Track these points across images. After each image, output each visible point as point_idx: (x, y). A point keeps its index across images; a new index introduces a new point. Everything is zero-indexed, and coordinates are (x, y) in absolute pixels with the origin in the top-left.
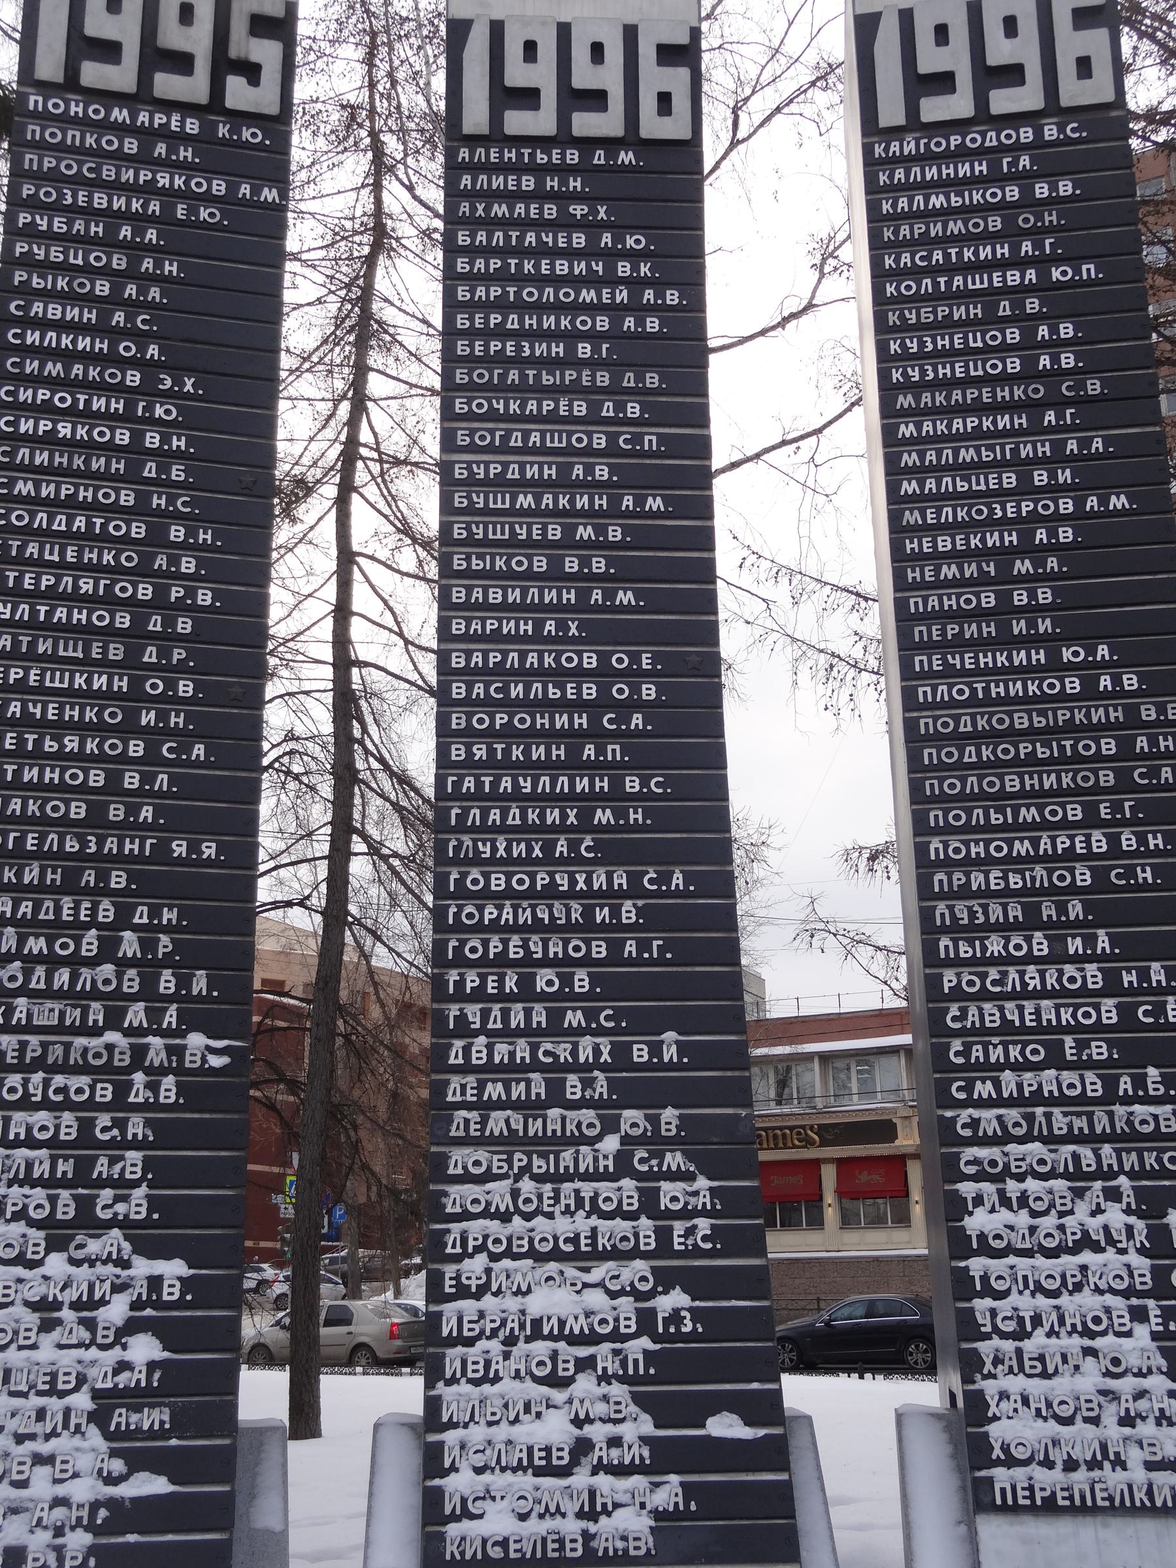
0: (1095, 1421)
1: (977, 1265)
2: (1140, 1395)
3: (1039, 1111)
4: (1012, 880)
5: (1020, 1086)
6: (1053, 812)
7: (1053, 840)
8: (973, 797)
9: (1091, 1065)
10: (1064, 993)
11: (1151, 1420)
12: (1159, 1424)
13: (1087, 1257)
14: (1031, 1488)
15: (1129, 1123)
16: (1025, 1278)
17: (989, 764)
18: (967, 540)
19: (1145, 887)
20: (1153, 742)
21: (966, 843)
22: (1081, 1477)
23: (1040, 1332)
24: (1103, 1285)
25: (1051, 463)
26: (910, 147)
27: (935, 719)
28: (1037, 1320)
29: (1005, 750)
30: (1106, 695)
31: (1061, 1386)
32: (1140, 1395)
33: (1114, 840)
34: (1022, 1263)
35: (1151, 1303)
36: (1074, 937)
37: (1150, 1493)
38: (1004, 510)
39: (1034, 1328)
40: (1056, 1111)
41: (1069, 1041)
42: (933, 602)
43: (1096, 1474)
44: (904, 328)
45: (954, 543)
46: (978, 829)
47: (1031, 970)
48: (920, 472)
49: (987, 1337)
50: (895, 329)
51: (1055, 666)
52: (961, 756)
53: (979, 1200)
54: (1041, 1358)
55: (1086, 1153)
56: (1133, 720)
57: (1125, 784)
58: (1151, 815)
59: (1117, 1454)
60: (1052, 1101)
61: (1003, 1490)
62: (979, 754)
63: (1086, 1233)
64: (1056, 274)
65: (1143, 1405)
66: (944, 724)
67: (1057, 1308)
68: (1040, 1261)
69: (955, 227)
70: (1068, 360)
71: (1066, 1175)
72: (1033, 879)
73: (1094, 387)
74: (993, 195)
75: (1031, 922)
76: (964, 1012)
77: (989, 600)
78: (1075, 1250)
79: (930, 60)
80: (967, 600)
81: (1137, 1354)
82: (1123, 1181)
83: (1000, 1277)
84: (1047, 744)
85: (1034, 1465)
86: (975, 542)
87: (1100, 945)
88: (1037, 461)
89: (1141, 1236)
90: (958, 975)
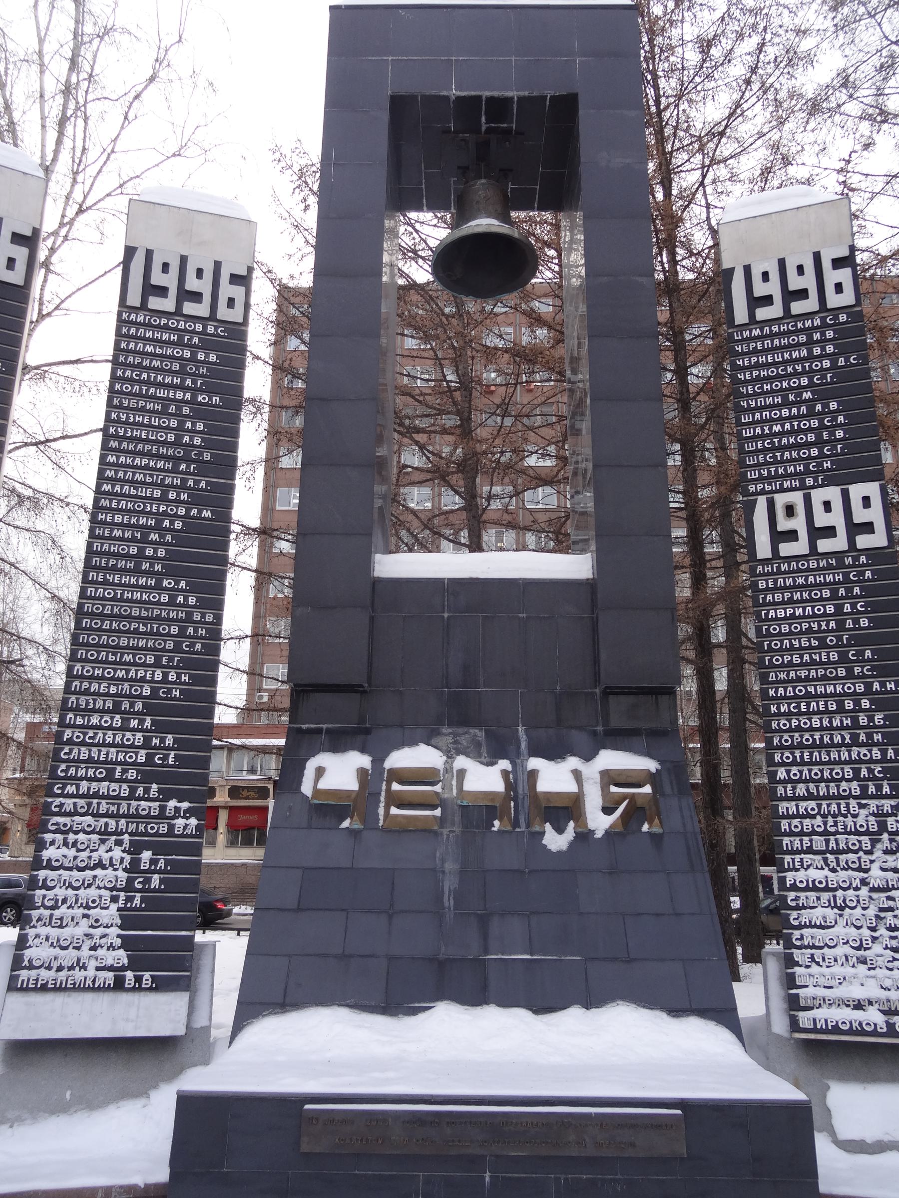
0: (78, 948)
1: (42, 874)
2: (104, 936)
3: (95, 801)
4: (112, 689)
5: (89, 789)
6: (140, 658)
7: (137, 671)
8: (103, 646)
9: (126, 781)
10: (122, 745)
11: (105, 948)
12: (108, 949)
13: (99, 872)
14: (37, 980)
15: (137, 809)
16: (65, 880)
17: (115, 631)
18: (130, 519)
19: (175, 699)
20: (196, 631)
21: (94, 668)
22: (63, 974)
23: (65, 906)
24: (101, 885)
25: (183, 487)
26: (141, 319)
27: (93, 605)
28: (64, 901)
29: (124, 625)
30: (180, 605)
31: (66, 932)
32: (104, 936)
33: (165, 675)
34: (65, 874)
35: (122, 894)
36: (134, 719)
37: (94, 981)
38: (151, 507)
39: (62, 904)
40: (104, 802)
41: (119, 769)
42: (106, 547)
43: (72, 972)
44: (121, 407)
45: (123, 519)
46: (101, 662)
47: (110, 733)
48: (113, 481)
49: (38, 908)
50: (116, 407)
51: (158, 587)
52: (102, 625)
53: (52, 843)
54: (61, 919)
55: (112, 823)
56: (189, 619)
57: (177, 649)
58: (186, 664)
59: (84, 963)
60: (103, 797)
61: (23, 981)
62: (111, 625)
63: (101, 860)
64: (200, 398)
65: (103, 941)
66: (97, 608)
67: (77, 895)
68: (75, 873)
69: (156, 364)
70: (197, 441)
71: (99, 833)
72: (122, 689)
73: (207, 456)
74: (177, 352)
75: (116, 709)
76: (71, 750)
77: (134, 550)
78: (92, 869)
79: (158, 278)
80: (123, 549)
81: (108, 917)
82: (126, 837)
83: (52, 880)
84: (145, 625)
85: (42, 969)
86: (133, 520)
87: (146, 724)
88: (172, 486)
89: (126, 864)
90: (73, 732)
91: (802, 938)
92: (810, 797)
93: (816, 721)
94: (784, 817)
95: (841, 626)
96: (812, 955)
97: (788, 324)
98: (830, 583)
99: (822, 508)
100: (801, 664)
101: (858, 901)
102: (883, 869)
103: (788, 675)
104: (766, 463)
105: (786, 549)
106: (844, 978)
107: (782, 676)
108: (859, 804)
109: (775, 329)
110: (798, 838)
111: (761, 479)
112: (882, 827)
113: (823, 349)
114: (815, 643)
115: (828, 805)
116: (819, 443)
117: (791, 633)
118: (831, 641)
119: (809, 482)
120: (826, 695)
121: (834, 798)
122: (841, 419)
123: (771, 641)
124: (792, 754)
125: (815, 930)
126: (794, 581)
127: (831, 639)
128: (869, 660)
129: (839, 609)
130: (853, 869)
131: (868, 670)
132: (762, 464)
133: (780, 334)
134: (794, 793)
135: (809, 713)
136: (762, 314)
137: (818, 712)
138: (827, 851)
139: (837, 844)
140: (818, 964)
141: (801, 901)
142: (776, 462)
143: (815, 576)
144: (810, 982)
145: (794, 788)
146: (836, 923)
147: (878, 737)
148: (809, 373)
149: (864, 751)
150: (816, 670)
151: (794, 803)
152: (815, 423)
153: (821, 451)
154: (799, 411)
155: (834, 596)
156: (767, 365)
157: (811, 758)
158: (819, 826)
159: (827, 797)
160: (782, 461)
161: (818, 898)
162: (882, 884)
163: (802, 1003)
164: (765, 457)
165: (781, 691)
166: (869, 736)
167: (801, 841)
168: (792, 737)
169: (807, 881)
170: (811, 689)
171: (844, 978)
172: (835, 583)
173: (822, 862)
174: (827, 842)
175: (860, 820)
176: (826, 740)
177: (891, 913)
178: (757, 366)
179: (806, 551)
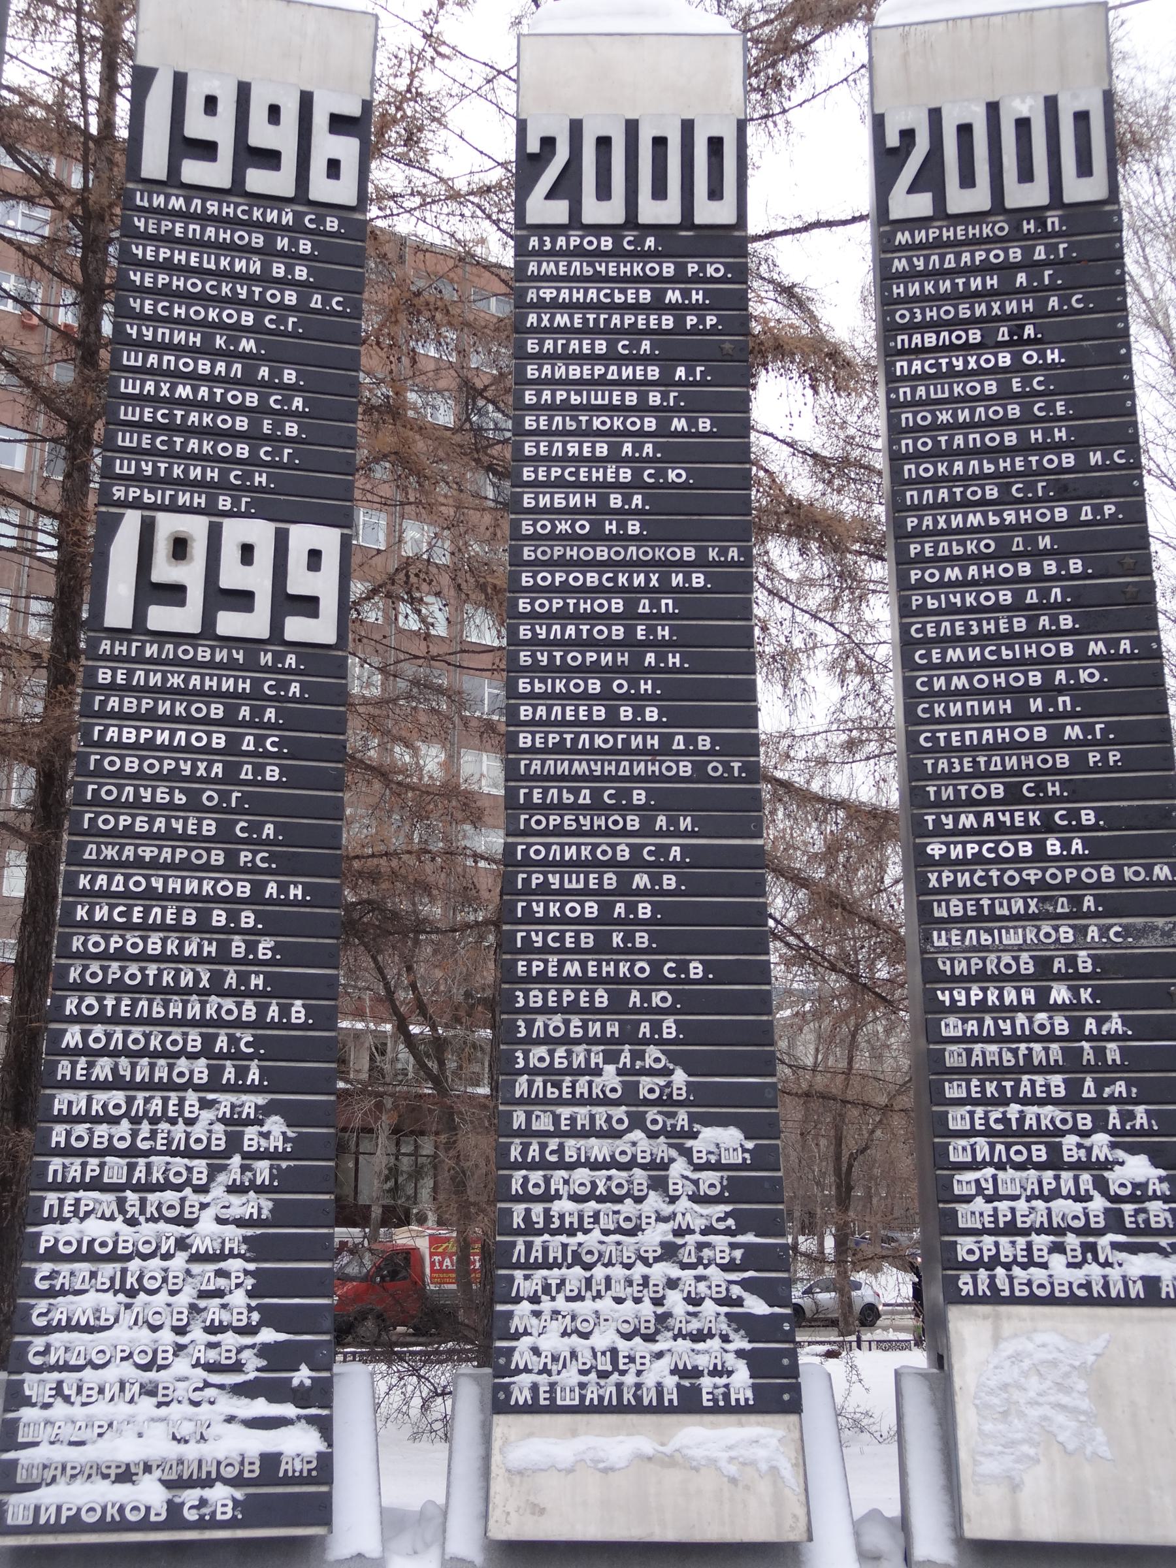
91: (46, 1352)
92: (117, 1083)
93: (154, 944)
94: (61, 1119)
95: (231, 775)
96: (60, 1383)
97: (237, 205)
98: (227, 695)
99: (238, 554)
100: (149, 836)
101: (165, 1280)
102: (220, 1221)
103: (120, 853)
104: (153, 452)
105: (160, 617)
106: (110, 1425)
107: (110, 853)
108: (201, 1100)
109: (213, 207)
110: (78, 1161)
111: (138, 478)
112: (234, 1143)
113: (290, 269)
114: (180, 798)
115: (147, 1101)
116: (253, 437)
117: (140, 775)
118: (210, 798)
119: (225, 503)
120: (181, 898)
121: (161, 1087)
122: (298, 403)
123: (101, 785)
124: (100, 1000)
125: (76, 1335)
126: (165, 679)
127: (210, 796)
128: (268, 842)
129: (234, 741)
130: (169, 1221)
131: (263, 860)
132: (146, 452)
133: (220, 221)
134: (88, 1075)
135: (145, 928)
136: (194, 171)
137: (162, 927)
138: (127, 1186)
139: (149, 1172)
140: (67, 1399)
141: (60, 1280)
142: (170, 454)
143: (203, 676)
144: (45, 1434)
145: (90, 1066)
146: (117, 1320)
147: (257, 981)
148: (259, 306)
149: (229, 1003)
150: (174, 848)
151: (84, 1094)
152: (252, 399)
153: (254, 451)
154: (228, 369)
155: (230, 719)
156: (186, 270)
157: (132, 1011)
158: (122, 1139)
159: (149, 1086)
160: (183, 455)
161: (93, 1275)
162: (211, 1246)
163: (21, 1477)
164: (153, 439)
165: (102, 880)
166: (243, 978)
167: (84, 1165)
168: (104, 969)
169: (80, 1243)
170: (158, 883)
171: (110, 1425)
172: (235, 695)
173: (114, 1206)
174: (131, 1168)
175: (199, 1131)
176: (167, 979)
177: (217, 1301)
178: (168, 266)
179: (196, 628)
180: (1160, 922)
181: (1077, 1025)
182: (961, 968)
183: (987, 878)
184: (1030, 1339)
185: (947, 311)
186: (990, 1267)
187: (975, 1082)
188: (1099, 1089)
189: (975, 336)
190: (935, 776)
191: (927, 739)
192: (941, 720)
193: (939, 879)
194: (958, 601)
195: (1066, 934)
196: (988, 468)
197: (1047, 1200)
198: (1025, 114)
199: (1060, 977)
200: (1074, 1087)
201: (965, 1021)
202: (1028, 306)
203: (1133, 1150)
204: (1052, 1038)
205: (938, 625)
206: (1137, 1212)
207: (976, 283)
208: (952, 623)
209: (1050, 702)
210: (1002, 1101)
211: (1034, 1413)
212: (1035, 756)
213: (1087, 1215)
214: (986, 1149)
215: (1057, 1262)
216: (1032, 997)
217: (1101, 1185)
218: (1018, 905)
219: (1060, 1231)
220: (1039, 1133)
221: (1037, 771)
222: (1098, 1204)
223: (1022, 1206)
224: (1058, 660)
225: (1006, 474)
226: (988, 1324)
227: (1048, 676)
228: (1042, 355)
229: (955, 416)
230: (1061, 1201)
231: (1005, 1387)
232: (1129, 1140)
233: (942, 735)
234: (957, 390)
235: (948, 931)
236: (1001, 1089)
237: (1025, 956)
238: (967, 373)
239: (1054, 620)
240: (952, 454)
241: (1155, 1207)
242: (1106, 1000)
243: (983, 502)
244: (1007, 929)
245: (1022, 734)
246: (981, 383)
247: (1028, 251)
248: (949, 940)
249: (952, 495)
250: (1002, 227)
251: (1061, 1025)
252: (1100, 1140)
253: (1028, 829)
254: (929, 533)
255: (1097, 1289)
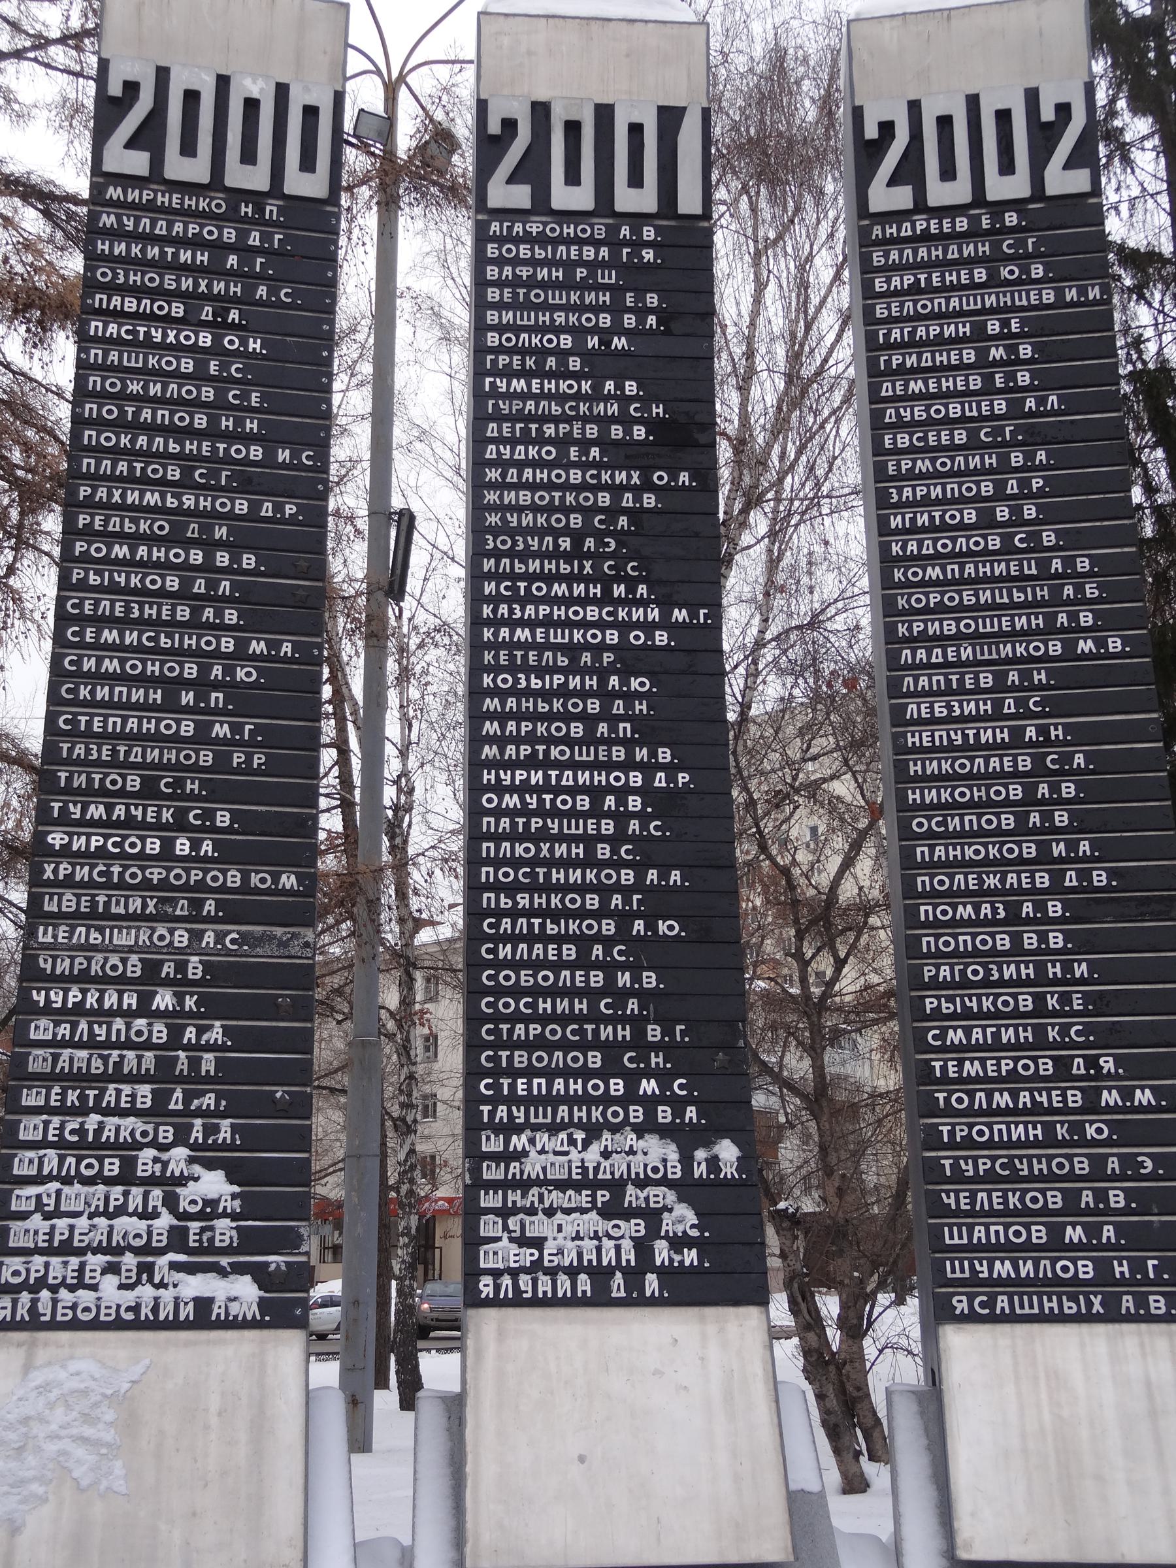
180: (278, 931)
181: (176, 1033)
182: (63, 966)
183: (107, 874)
184: (64, 1367)
185: (151, 278)
186: (35, 1289)
187: (57, 1089)
188: (187, 1101)
189: (178, 310)
190: (69, 762)
191: (66, 722)
192: (85, 703)
193: (55, 871)
194: (122, 580)
195: (181, 938)
196: (174, 448)
197: (110, 1216)
198: (255, 94)
199: (167, 983)
200: (161, 1098)
201: (57, 1024)
202: (236, 289)
203: (210, 1165)
204: (148, 1045)
205: (97, 603)
206: (203, 1230)
207: (185, 256)
208: (113, 602)
209: (201, 697)
210: (82, 1110)
211: (52, 1447)
212: (179, 751)
213: (150, 1233)
214: (55, 1162)
215: (109, 1284)
216: (134, 1002)
217: (171, 1202)
218: (136, 905)
219: (119, 1251)
220: (115, 1146)
221: (178, 767)
222: (165, 1221)
223: (82, 1223)
224: (217, 654)
225: (190, 457)
226: (21, 1353)
227: (204, 670)
228: (244, 342)
229: (145, 388)
230: (125, 1219)
231: (26, 1420)
232: (207, 1156)
233: (83, 719)
234: (152, 361)
235: (55, 926)
236: (83, 1098)
237: (134, 958)
238: (164, 347)
239: (219, 614)
240: (136, 427)
241: (223, 1224)
242: (211, 1008)
243: (163, 482)
244: (120, 929)
245: (168, 727)
246: (178, 359)
247: (243, 235)
248: (55, 936)
249: (131, 469)
250: (218, 204)
251: (160, 1032)
252: (180, 1153)
253: (159, 826)
254: (101, 505)
255: (145, 1311)
